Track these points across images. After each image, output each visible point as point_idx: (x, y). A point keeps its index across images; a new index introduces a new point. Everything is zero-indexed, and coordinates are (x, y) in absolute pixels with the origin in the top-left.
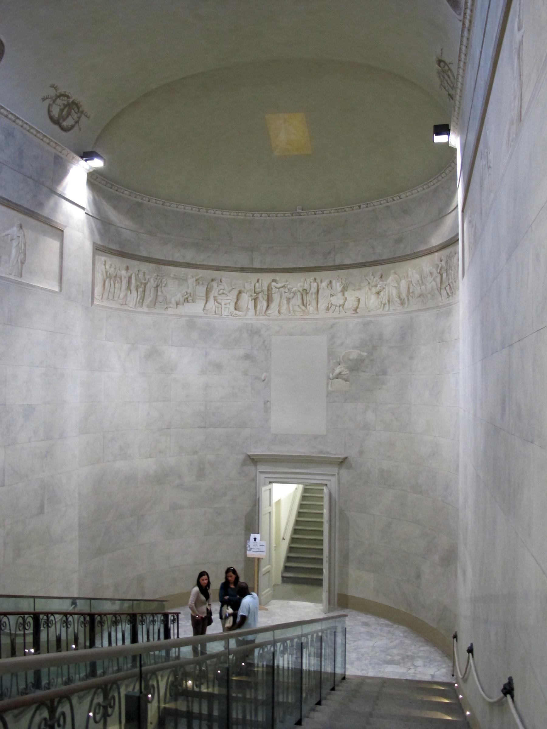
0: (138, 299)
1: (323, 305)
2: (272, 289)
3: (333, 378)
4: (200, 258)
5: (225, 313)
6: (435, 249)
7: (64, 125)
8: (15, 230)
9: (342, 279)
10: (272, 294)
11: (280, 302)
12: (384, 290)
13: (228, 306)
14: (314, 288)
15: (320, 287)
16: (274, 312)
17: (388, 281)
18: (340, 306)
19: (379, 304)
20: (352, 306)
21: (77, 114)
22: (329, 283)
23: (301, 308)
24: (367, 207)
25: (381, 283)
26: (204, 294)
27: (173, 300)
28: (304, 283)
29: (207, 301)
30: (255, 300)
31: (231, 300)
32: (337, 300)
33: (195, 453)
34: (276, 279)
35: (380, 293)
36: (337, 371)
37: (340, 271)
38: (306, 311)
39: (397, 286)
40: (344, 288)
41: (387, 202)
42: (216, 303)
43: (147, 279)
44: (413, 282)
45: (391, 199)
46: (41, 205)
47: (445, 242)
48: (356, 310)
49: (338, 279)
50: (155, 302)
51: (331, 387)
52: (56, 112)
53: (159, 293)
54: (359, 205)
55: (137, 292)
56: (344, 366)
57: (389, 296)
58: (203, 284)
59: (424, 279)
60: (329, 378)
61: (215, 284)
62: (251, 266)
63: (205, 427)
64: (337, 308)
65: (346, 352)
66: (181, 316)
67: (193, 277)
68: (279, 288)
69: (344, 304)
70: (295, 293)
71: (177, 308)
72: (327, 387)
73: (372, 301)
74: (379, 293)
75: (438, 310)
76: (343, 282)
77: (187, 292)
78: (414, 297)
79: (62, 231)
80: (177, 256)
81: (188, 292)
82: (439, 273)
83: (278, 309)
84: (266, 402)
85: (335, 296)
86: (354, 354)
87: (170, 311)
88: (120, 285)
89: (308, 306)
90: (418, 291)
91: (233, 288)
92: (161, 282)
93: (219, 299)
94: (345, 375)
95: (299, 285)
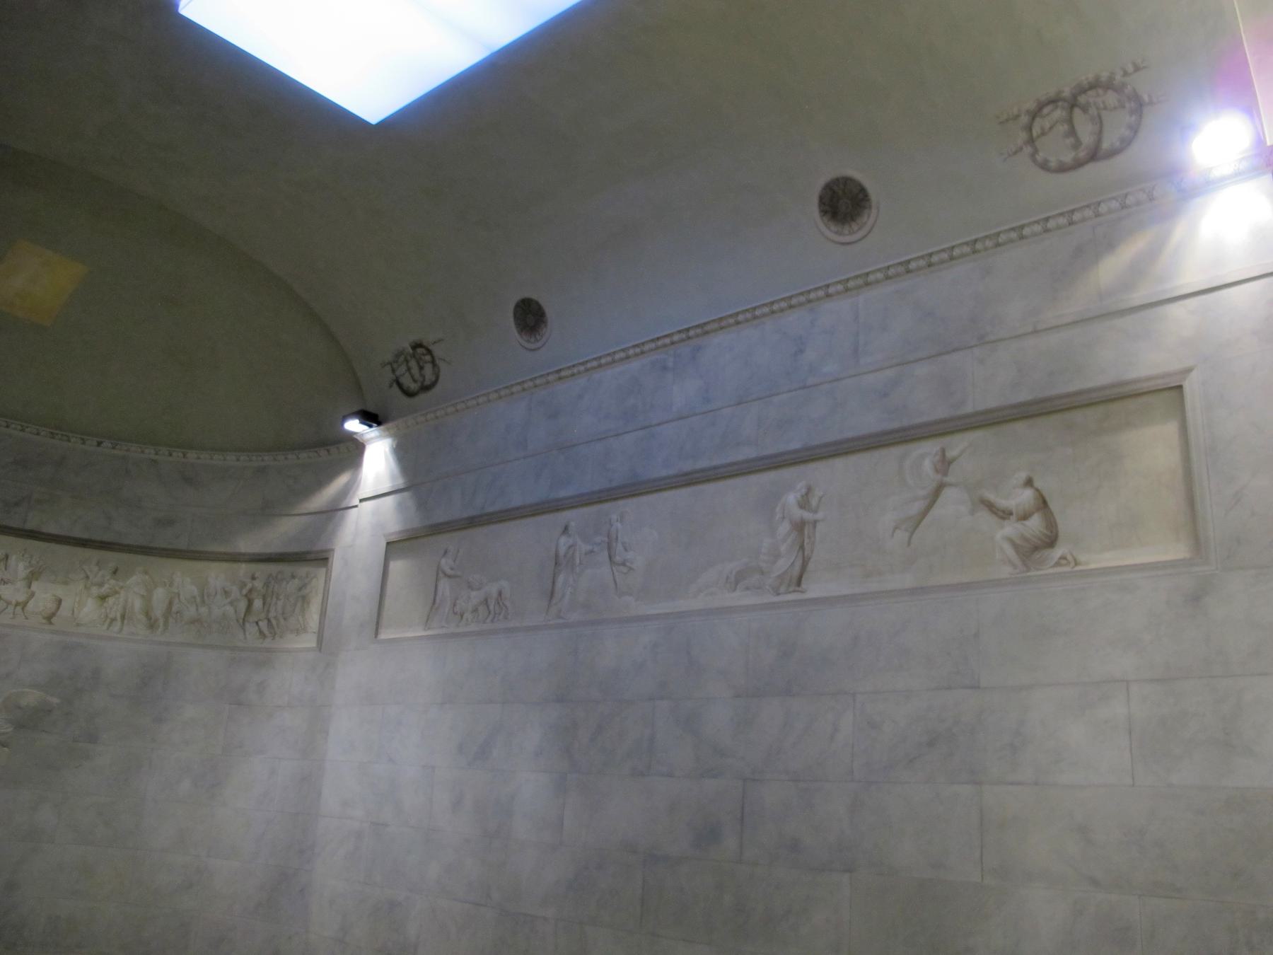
12: (117, 596)
17: (128, 583)
19: (102, 617)
22: (4, 559)
24: (114, 448)
25: (112, 582)
39: (145, 594)
40: (32, 573)
41: (157, 454)
44: (181, 597)
47: (271, 554)
48: (49, 618)
49: (23, 556)
54: (99, 440)
57: (125, 608)
64: (10, 609)
69: (25, 604)
73: (86, 610)
76: (34, 562)
82: (246, 596)
85: (10, 584)
86: (32, 698)
90: (191, 612)
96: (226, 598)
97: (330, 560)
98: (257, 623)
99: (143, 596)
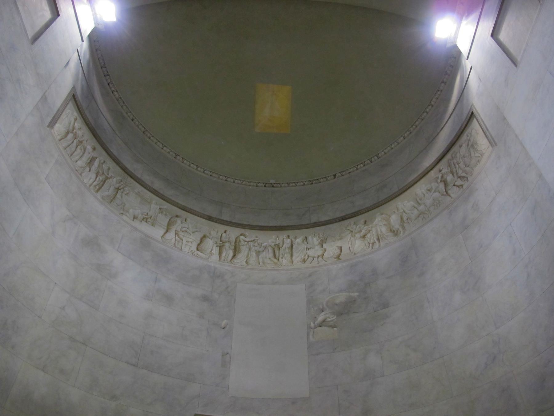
0: (95, 183)
1: (298, 257)
2: (240, 241)
3: (315, 327)
4: (169, 193)
5: (186, 249)
6: (429, 169)
9: (319, 234)
10: (239, 245)
11: (248, 254)
12: (371, 232)
13: (190, 244)
14: (288, 244)
15: (293, 243)
16: (241, 262)
17: (374, 223)
18: (318, 257)
19: (367, 245)
20: (333, 255)
22: (305, 239)
23: (272, 260)
24: (342, 175)
25: (366, 227)
26: (166, 223)
27: (131, 211)
28: (276, 239)
29: (167, 231)
30: (221, 247)
31: (194, 240)
32: (316, 251)
33: (114, 397)
34: (245, 233)
35: (366, 236)
36: (320, 318)
37: (315, 228)
38: (278, 263)
39: (386, 223)
40: (322, 241)
42: (177, 237)
43: (110, 175)
45: (369, 161)
48: (338, 257)
49: (314, 235)
50: (112, 199)
51: (313, 337)
53: (118, 196)
55: (97, 177)
56: (328, 312)
57: (377, 235)
58: (166, 215)
59: (421, 200)
60: (309, 327)
61: (179, 221)
62: (219, 217)
63: (136, 366)
64: (316, 259)
65: (330, 297)
66: (136, 229)
67: (157, 205)
68: (248, 242)
70: (265, 248)
71: (133, 220)
72: (308, 338)
74: (365, 236)
75: (450, 207)
76: (321, 236)
77: (148, 214)
78: (412, 221)
80: (147, 178)
81: (149, 214)
82: (441, 181)
83: (245, 260)
84: (224, 355)
86: (342, 298)
87: (124, 217)
88: (82, 154)
89: (280, 259)
90: (416, 212)
91: (197, 231)
92: (123, 188)
93: (181, 235)
94: (331, 321)
95: (270, 241)
96: (431, 192)
97: (475, 112)
98: (454, 185)
99: (385, 225)
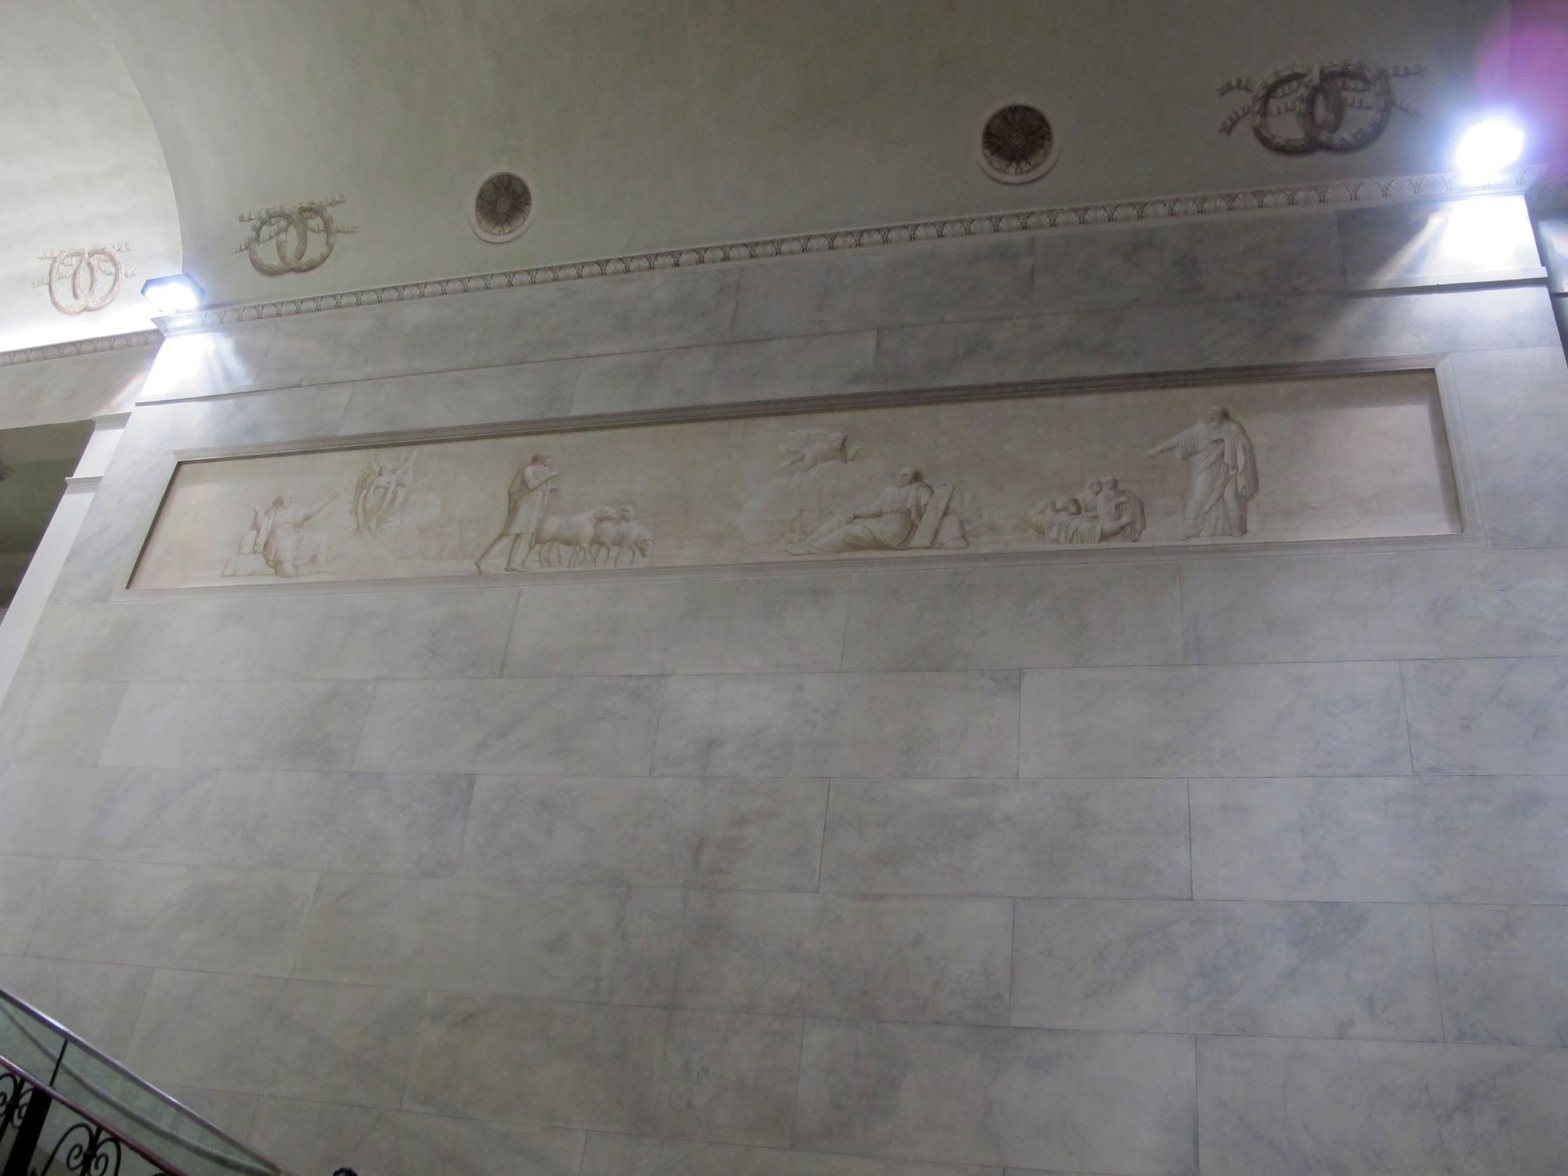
7: (1343, 139)
8: (1200, 431)
21: (1369, 89)
46: (1300, 340)
52: (1288, 128)
79: (1432, 371)
